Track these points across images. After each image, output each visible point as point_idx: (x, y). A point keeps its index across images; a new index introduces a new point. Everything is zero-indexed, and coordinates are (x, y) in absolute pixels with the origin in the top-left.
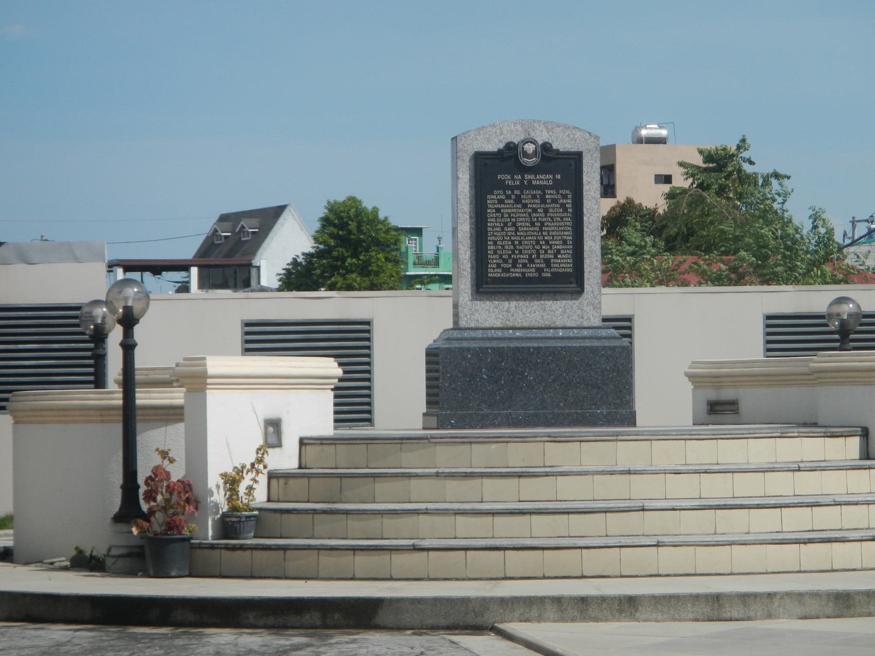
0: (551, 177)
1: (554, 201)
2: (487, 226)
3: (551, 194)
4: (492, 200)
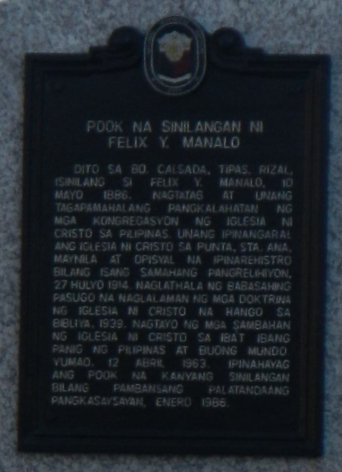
0: (236, 126)
1: (243, 195)
2: (51, 265)
3: (234, 176)
4: (65, 191)
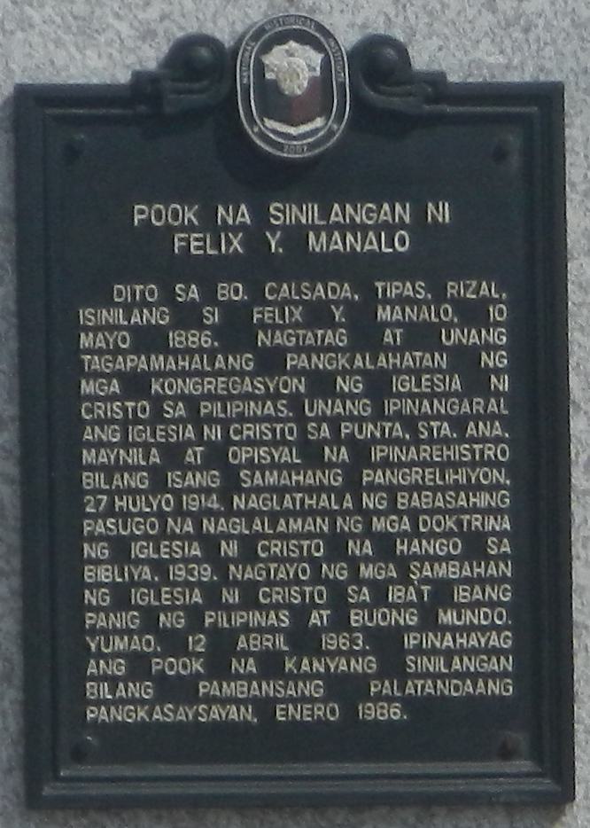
0: (404, 212)
1: (422, 336)
4: (102, 330)
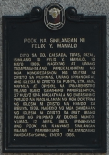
0: (75, 40)
1: (78, 64)
3: (75, 57)
